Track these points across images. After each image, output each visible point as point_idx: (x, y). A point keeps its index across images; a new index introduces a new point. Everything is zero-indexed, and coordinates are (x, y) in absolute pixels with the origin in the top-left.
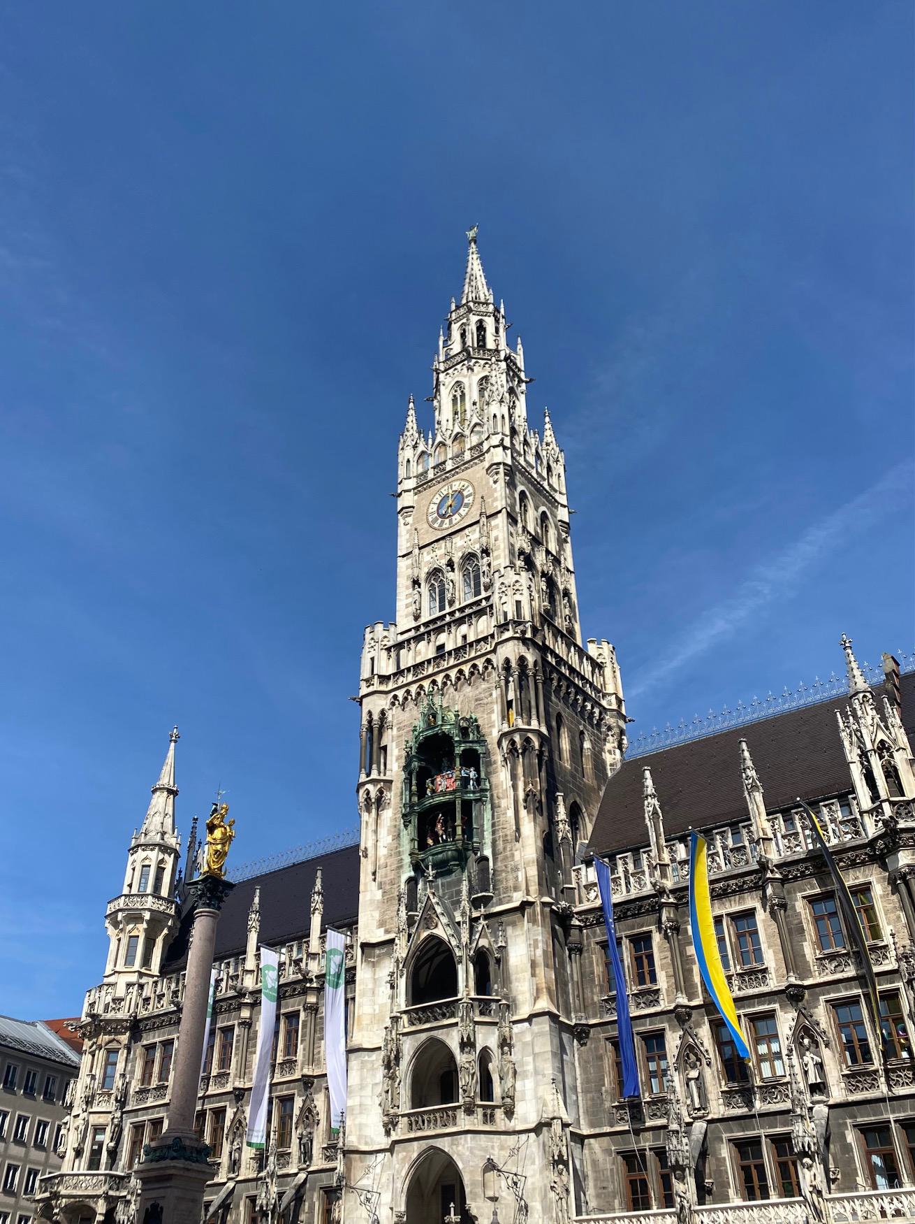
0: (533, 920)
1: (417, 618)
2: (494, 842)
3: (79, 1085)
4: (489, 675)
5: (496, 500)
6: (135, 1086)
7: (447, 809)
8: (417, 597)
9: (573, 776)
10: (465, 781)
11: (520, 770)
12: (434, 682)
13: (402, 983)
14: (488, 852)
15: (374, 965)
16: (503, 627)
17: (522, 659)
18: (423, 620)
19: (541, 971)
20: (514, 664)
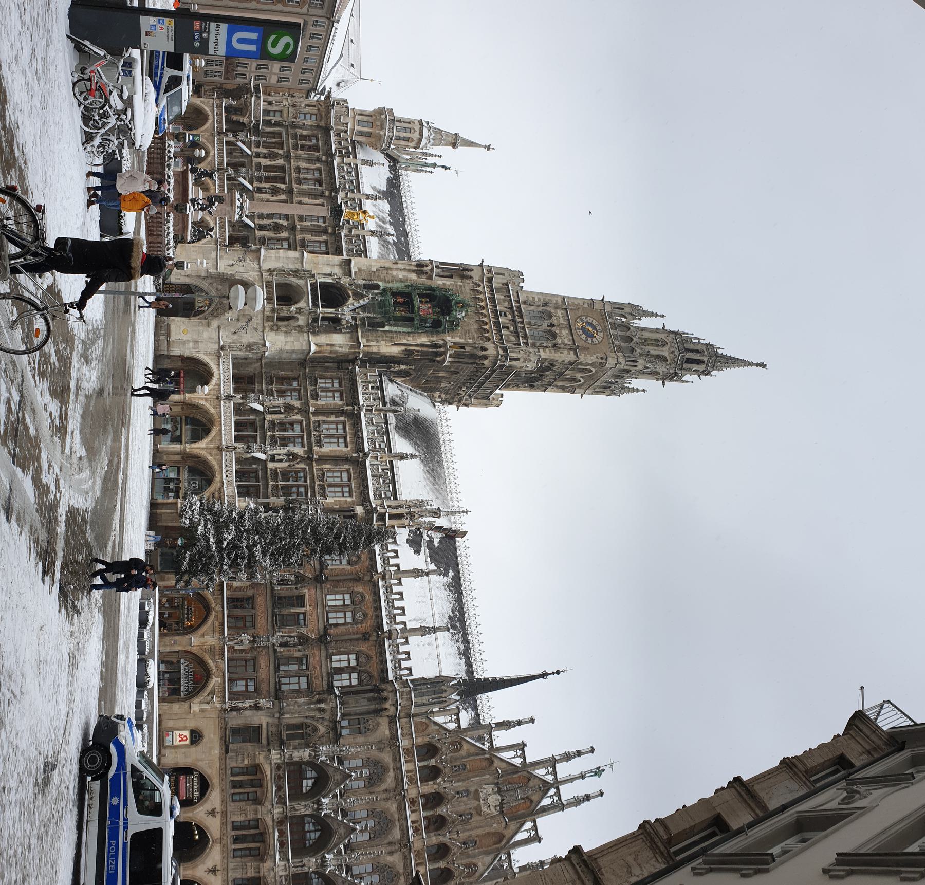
0: (352, 347)
1: (525, 303)
2: (391, 332)
3: (301, 99)
4: (482, 339)
5: (586, 355)
6: (299, 131)
7: (412, 310)
8: (537, 304)
9: (425, 375)
10: (425, 321)
11: (425, 349)
12: (483, 308)
13: (330, 280)
14: (387, 328)
15: (340, 265)
16: (505, 350)
17: (486, 357)
18: (522, 306)
19: (329, 348)
20: (484, 353)
